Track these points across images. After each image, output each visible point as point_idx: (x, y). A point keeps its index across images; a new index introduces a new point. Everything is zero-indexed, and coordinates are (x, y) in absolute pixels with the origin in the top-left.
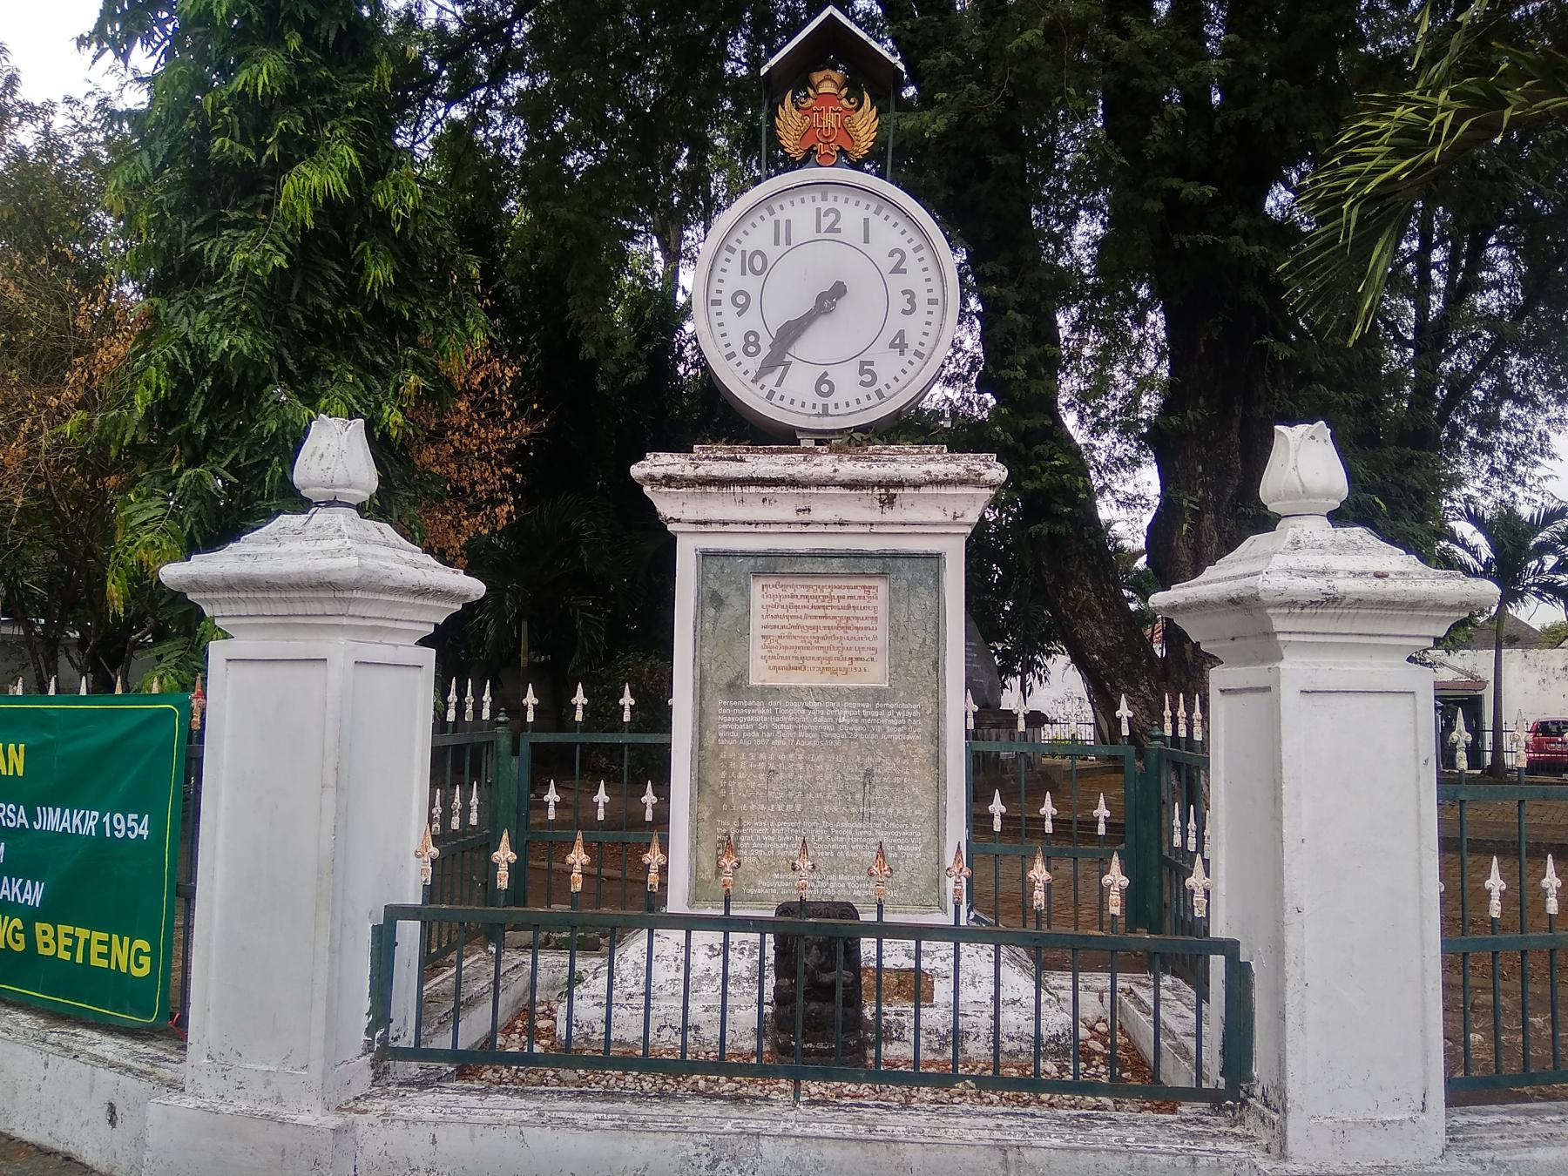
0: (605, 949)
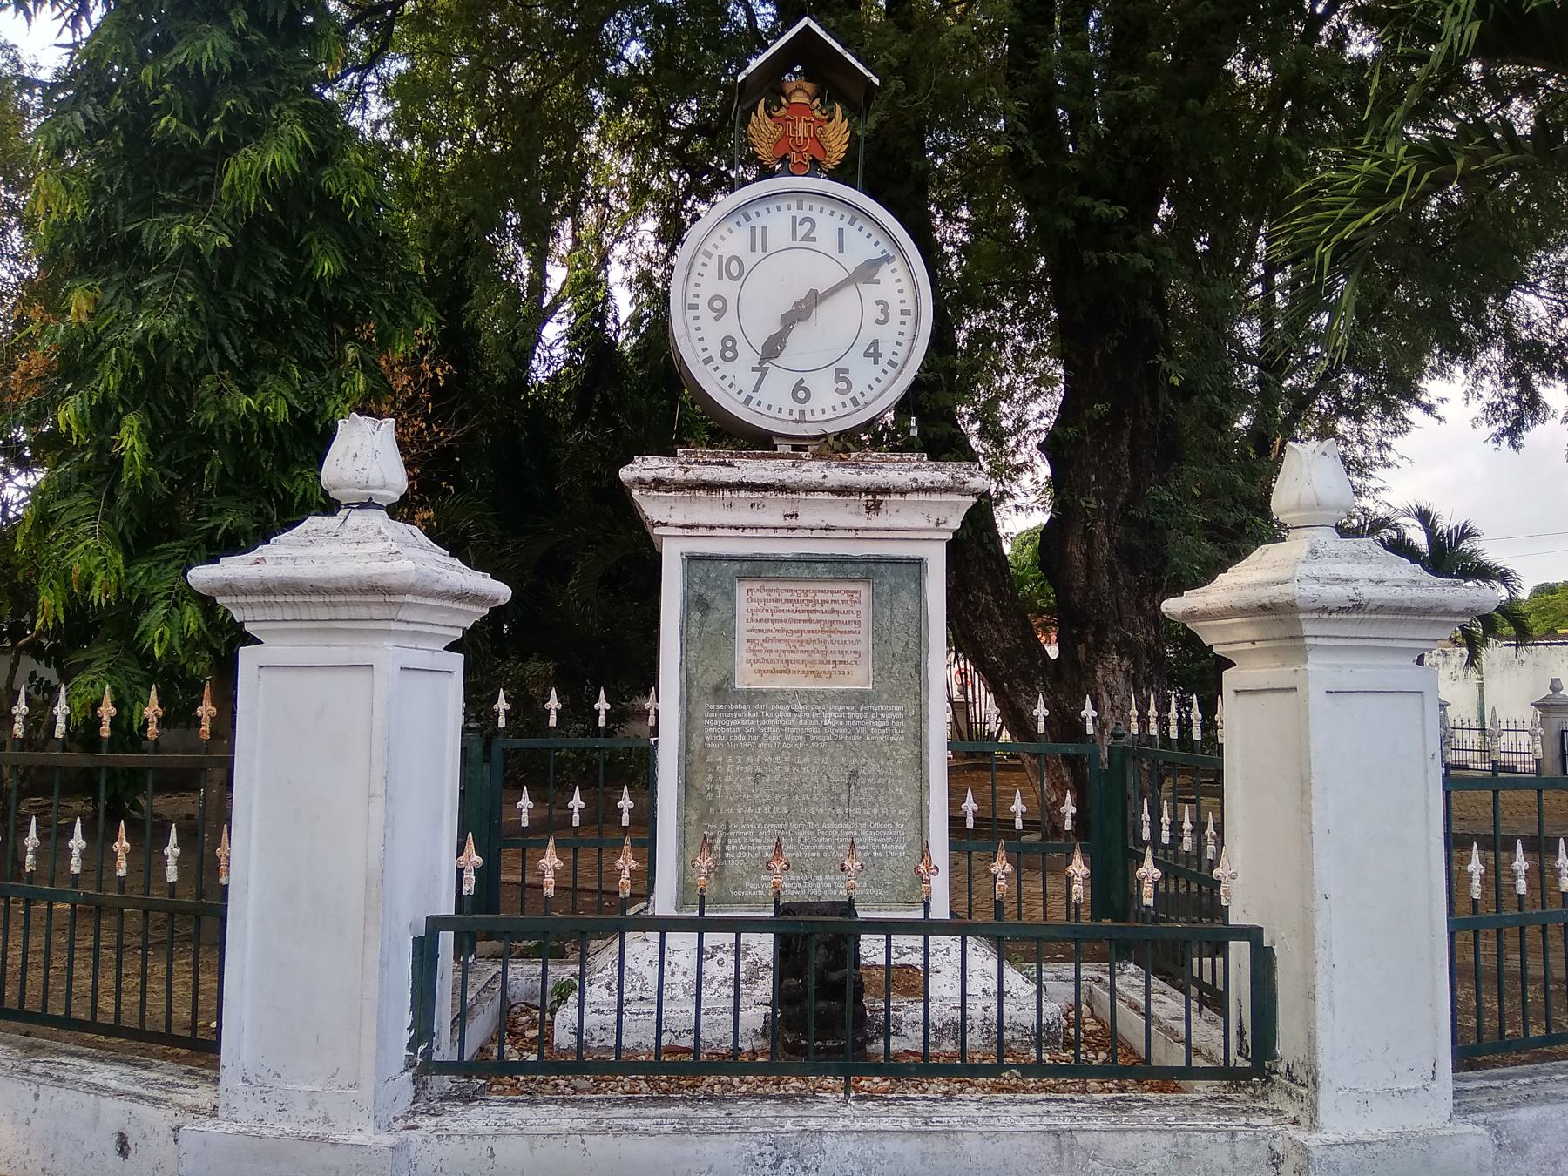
0: (576, 956)
